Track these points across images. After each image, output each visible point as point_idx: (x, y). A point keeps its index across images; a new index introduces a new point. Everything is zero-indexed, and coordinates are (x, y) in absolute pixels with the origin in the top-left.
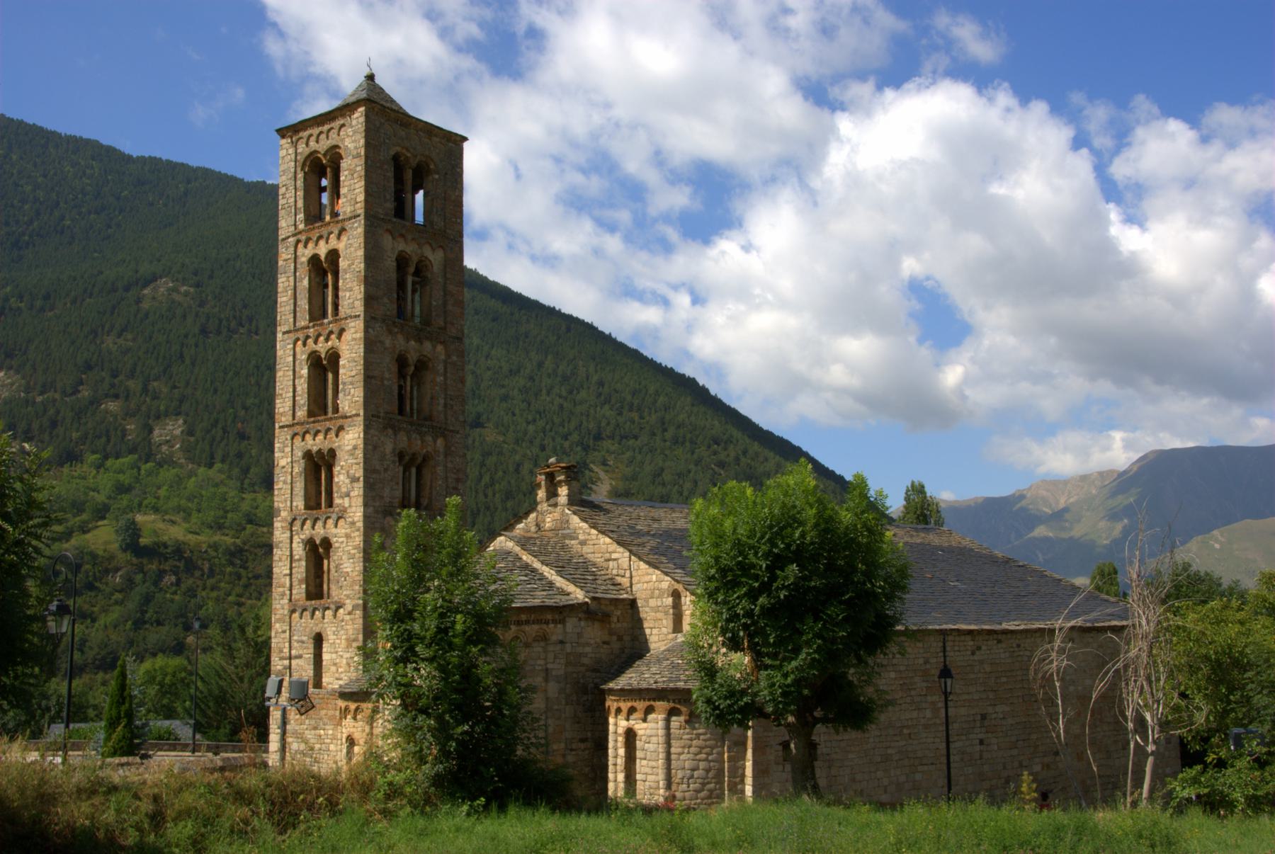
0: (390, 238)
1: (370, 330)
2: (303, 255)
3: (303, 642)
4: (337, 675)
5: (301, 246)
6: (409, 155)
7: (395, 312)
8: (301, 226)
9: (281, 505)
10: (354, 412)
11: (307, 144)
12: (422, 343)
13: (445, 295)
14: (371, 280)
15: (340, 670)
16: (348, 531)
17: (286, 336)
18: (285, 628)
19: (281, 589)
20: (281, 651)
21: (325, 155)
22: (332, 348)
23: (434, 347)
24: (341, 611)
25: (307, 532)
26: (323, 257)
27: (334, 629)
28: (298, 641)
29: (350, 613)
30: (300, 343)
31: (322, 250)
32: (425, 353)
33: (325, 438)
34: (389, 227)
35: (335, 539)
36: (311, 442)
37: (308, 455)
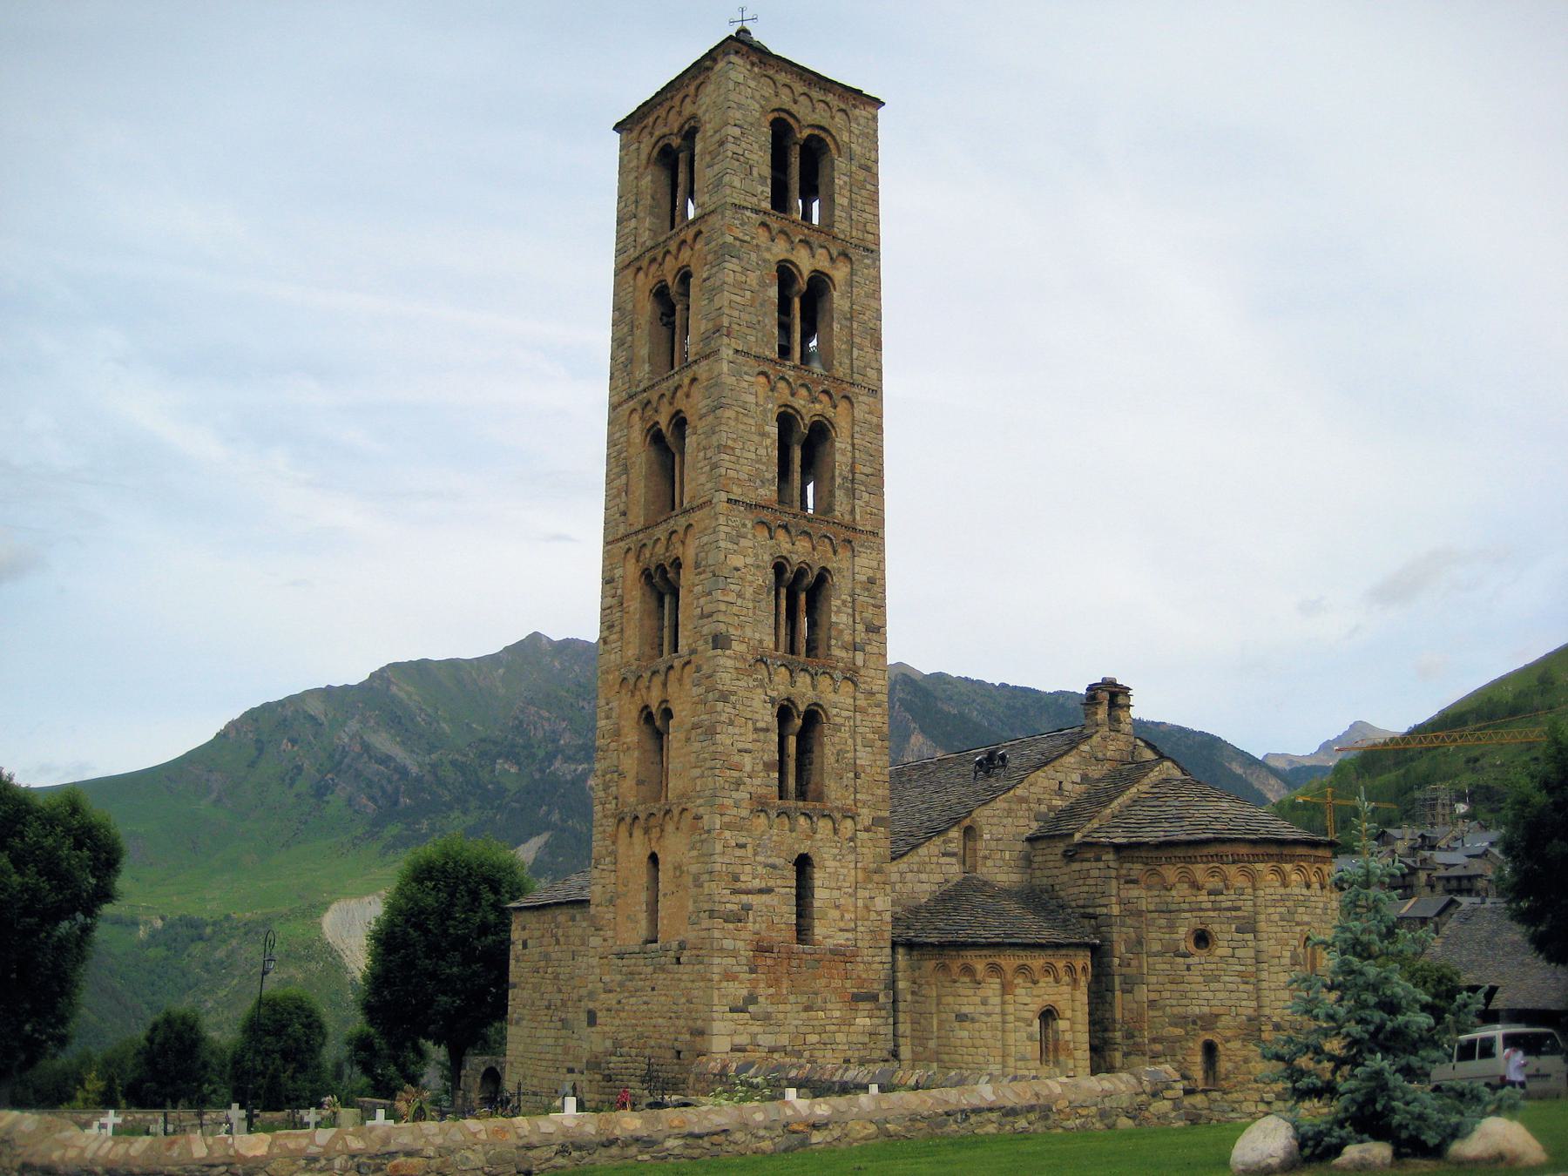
2: (768, 250)
3: (774, 867)
4: (842, 925)
8: (767, 205)
9: (732, 631)
10: (869, 528)
15: (847, 916)
16: (861, 702)
17: (740, 359)
18: (742, 840)
19: (735, 774)
20: (736, 879)
24: (849, 823)
25: (781, 685)
27: (836, 851)
28: (766, 865)
29: (867, 830)
31: (806, 263)
33: (814, 549)
35: (835, 711)
36: (789, 546)
37: (779, 568)
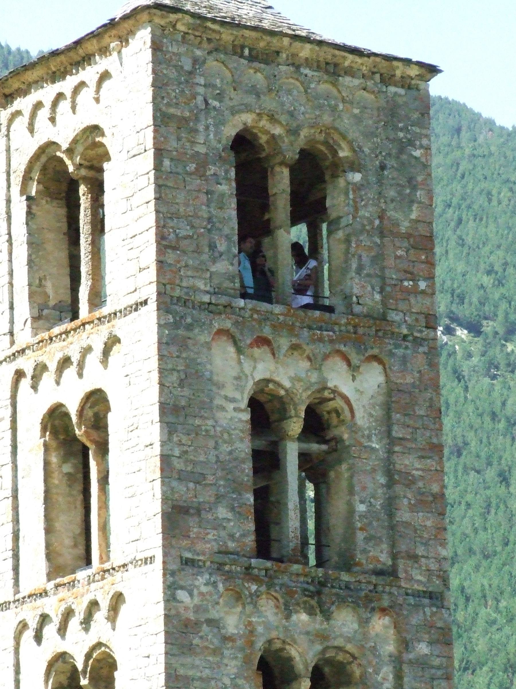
0: (232, 349)
1: (182, 595)
5: (25, 383)
6: (278, 131)
7: (250, 541)
11: (31, 128)
12: (327, 616)
13: (390, 484)
14: (178, 464)
21: (70, 151)
22: (99, 644)
23: (364, 622)
26: (73, 409)
30: (29, 635)
32: (339, 642)
34: (228, 324)
